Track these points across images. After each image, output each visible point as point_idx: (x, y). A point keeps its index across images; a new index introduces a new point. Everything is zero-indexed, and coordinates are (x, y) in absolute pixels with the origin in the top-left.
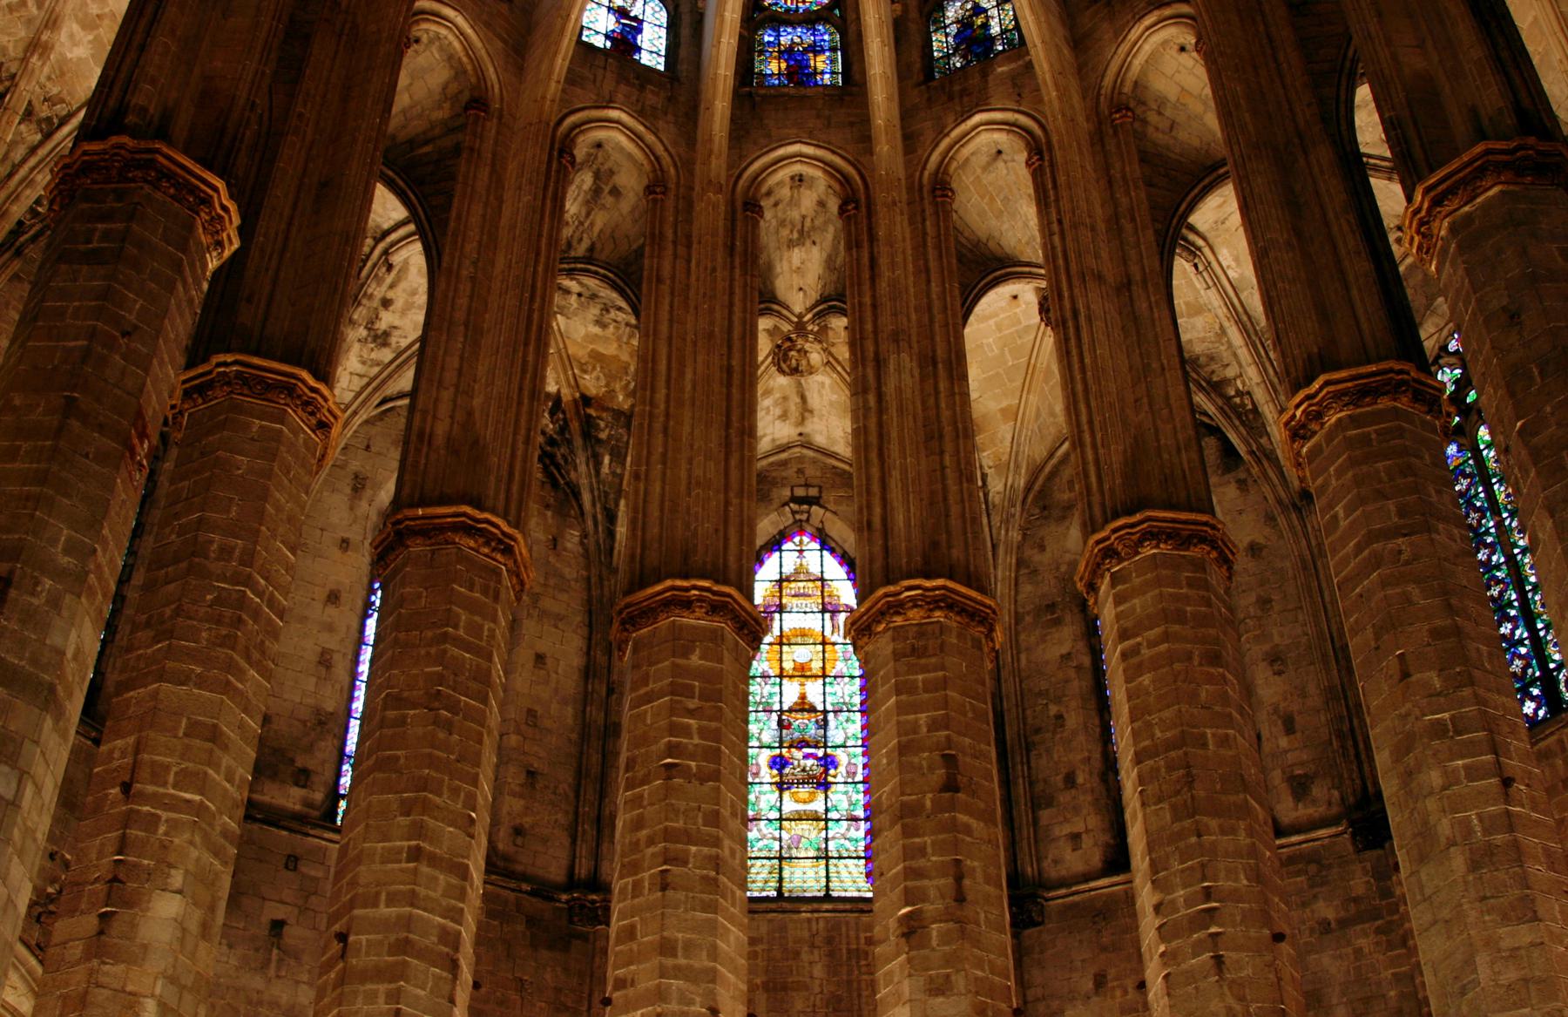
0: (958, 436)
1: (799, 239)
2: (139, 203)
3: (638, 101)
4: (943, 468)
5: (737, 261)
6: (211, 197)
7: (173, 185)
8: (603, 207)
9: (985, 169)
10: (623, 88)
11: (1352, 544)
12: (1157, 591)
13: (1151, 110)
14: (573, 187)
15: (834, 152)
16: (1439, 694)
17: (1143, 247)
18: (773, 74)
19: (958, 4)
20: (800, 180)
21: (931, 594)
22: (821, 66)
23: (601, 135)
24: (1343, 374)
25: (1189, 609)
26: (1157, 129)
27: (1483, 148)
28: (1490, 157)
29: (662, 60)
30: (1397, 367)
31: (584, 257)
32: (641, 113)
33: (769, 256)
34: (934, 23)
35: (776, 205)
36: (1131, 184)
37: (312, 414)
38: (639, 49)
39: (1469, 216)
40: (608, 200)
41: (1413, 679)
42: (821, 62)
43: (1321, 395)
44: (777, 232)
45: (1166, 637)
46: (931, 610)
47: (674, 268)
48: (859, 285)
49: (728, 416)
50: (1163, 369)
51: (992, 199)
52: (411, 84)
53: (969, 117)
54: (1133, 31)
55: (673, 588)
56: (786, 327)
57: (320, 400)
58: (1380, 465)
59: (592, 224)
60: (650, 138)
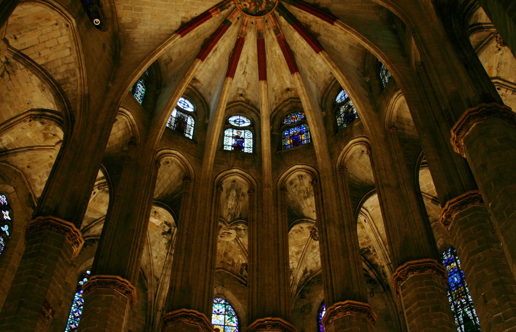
0: (353, 250)
1: (307, 196)
2: (46, 236)
3: (242, 164)
4: (349, 262)
5: (279, 208)
6: (70, 229)
7: (56, 228)
8: (241, 201)
9: (360, 158)
10: (237, 161)
11: (465, 259)
12: (414, 289)
13: (405, 125)
14: (231, 196)
15: (307, 165)
16: (497, 307)
17: (402, 172)
18: (288, 145)
19: (344, 107)
20: (302, 177)
21: (345, 306)
22: (303, 138)
23: (232, 178)
24: (454, 200)
25: (426, 293)
26: (409, 130)
27: (468, 111)
28: (471, 114)
29: (251, 149)
30: (472, 192)
31: (239, 218)
32: (243, 168)
33: (298, 203)
34: (337, 115)
35: (296, 186)
36: (397, 151)
37: (123, 289)
38: (243, 148)
39: (468, 135)
40: (242, 198)
41: (488, 303)
42: (303, 137)
43: (449, 209)
44: (299, 195)
45: (419, 305)
46: (345, 312)
47: (258, 215)
48: (319, 207)
49: (278, 261)
50: (412, 211)
51: (365, 167)
52: (170, 176)
53: (348, 143)
54: (391, 101)
55: (259, 322)
56: (312, 225)
57: (125, 284)
58: (471, 228)
59: (239, 207)
60: (247, 175)
